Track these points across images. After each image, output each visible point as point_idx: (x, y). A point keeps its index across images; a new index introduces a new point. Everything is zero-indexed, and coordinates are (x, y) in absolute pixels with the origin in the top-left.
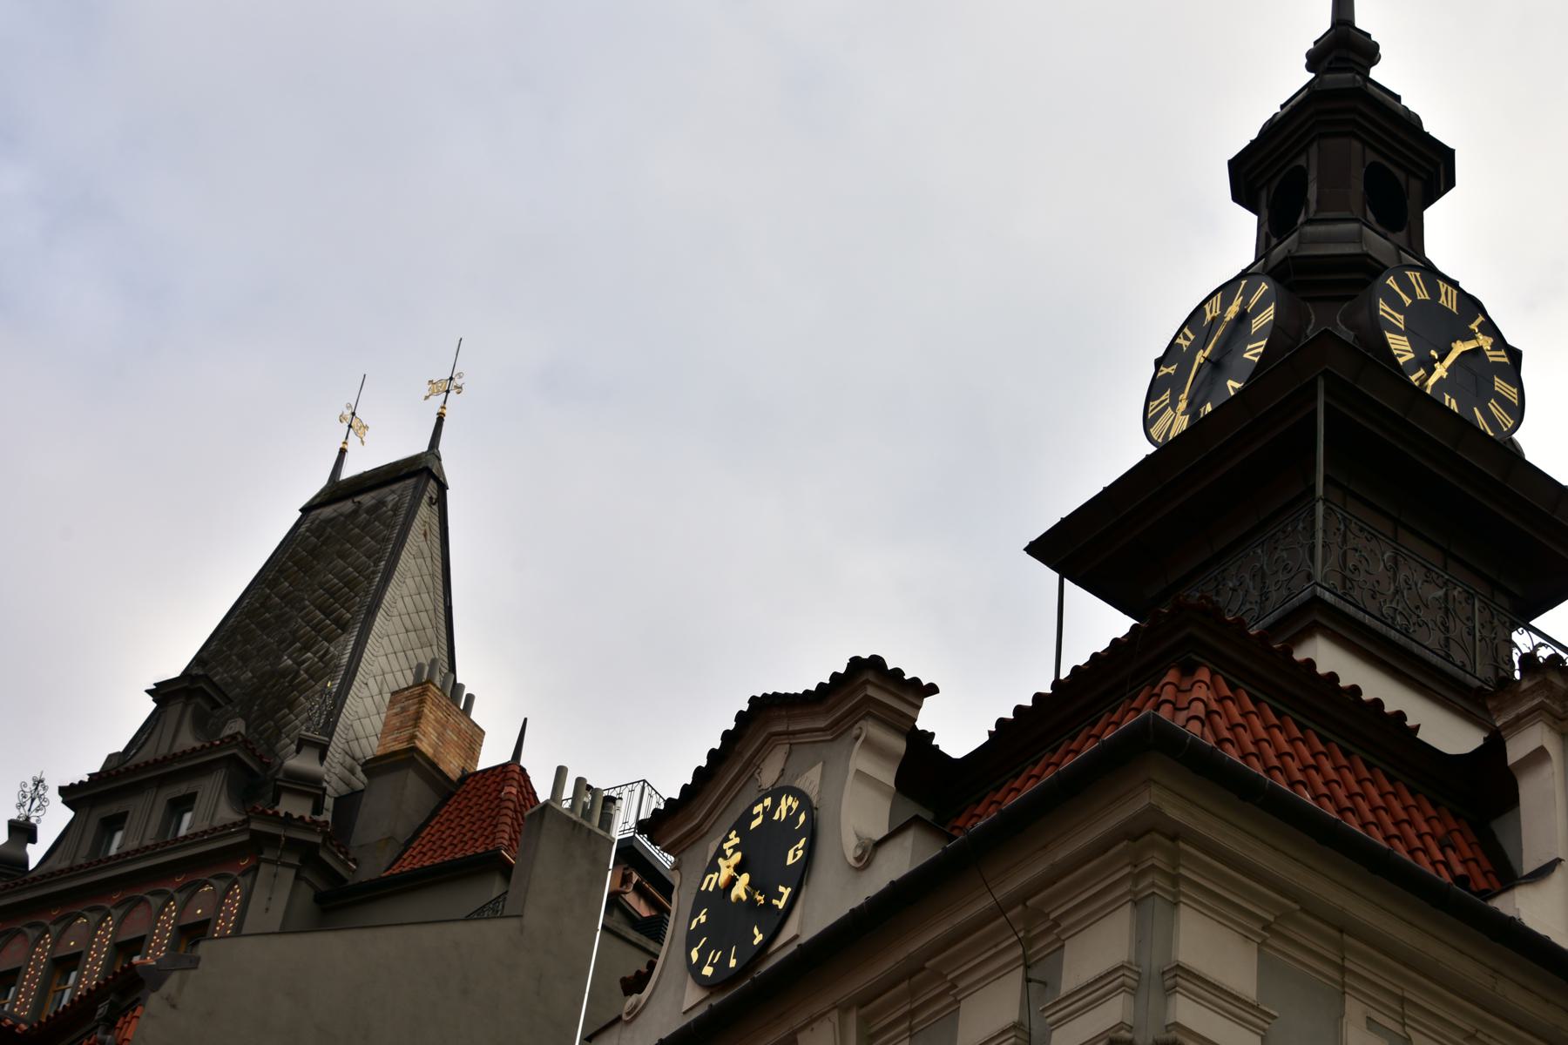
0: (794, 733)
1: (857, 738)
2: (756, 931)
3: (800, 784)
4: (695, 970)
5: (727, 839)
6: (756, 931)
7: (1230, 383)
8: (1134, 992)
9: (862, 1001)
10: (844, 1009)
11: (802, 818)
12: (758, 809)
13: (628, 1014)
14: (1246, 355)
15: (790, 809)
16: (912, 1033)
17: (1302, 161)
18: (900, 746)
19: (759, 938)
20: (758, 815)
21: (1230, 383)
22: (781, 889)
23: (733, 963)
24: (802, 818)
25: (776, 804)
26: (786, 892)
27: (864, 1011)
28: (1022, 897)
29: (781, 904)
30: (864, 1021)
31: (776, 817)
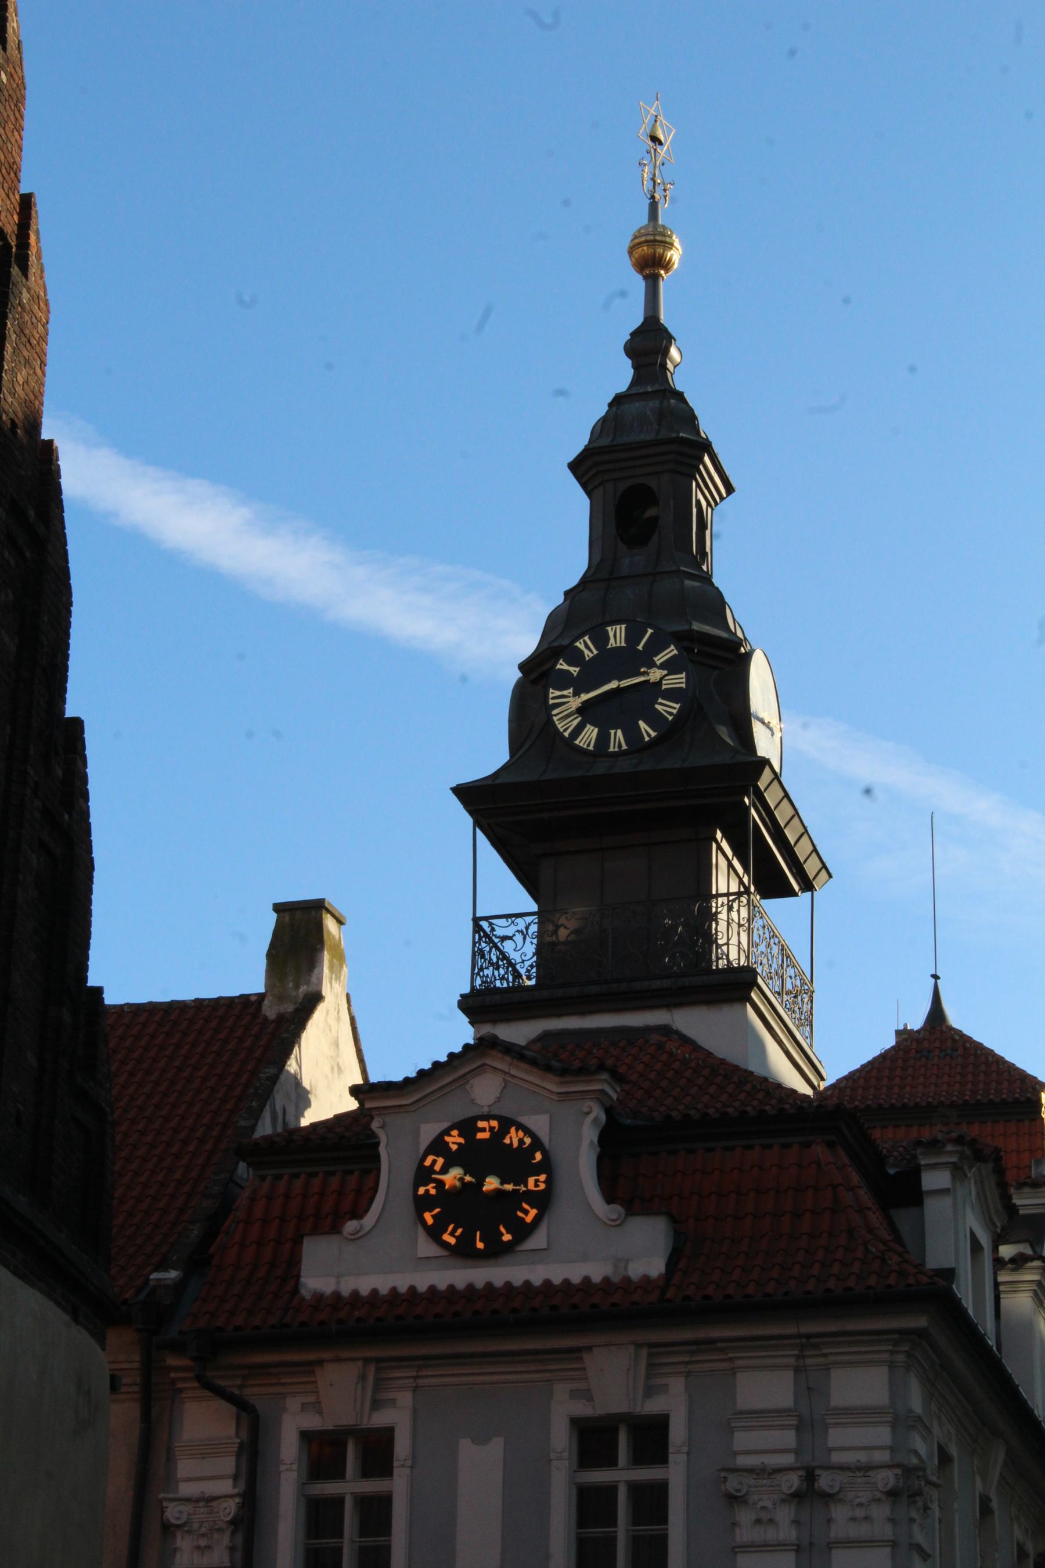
0: (513, 1076)
1: (588, 1113)
2: (503, 1230)
3: (523, 1120)
4: (435, 1233)
5: (447, 1132)
6: (503, 1230)
7: (642, 725)
8: (894, 1425)
9: (651, 1345)
10: (639, 1346)
11: (538, 1156)
12: (481, 1124)
13: (352, 1234)
14: (657, 707)
15: (521, 1142)
16: (688, 1374)
17: (653, 483)
18: (603, 1117)
19: (507, 1237)
20: (483, 1130)
21: (642, 725)
22: (526, 1206)
23: (480, 1245)
24: (538, 1156)
25: (504, 1130)
26: (533, 1212)
27: (654, 1350)
28: (808, 1336)
29: (529, 1219)
30: (650, 1355)
31: (507, 1141)
